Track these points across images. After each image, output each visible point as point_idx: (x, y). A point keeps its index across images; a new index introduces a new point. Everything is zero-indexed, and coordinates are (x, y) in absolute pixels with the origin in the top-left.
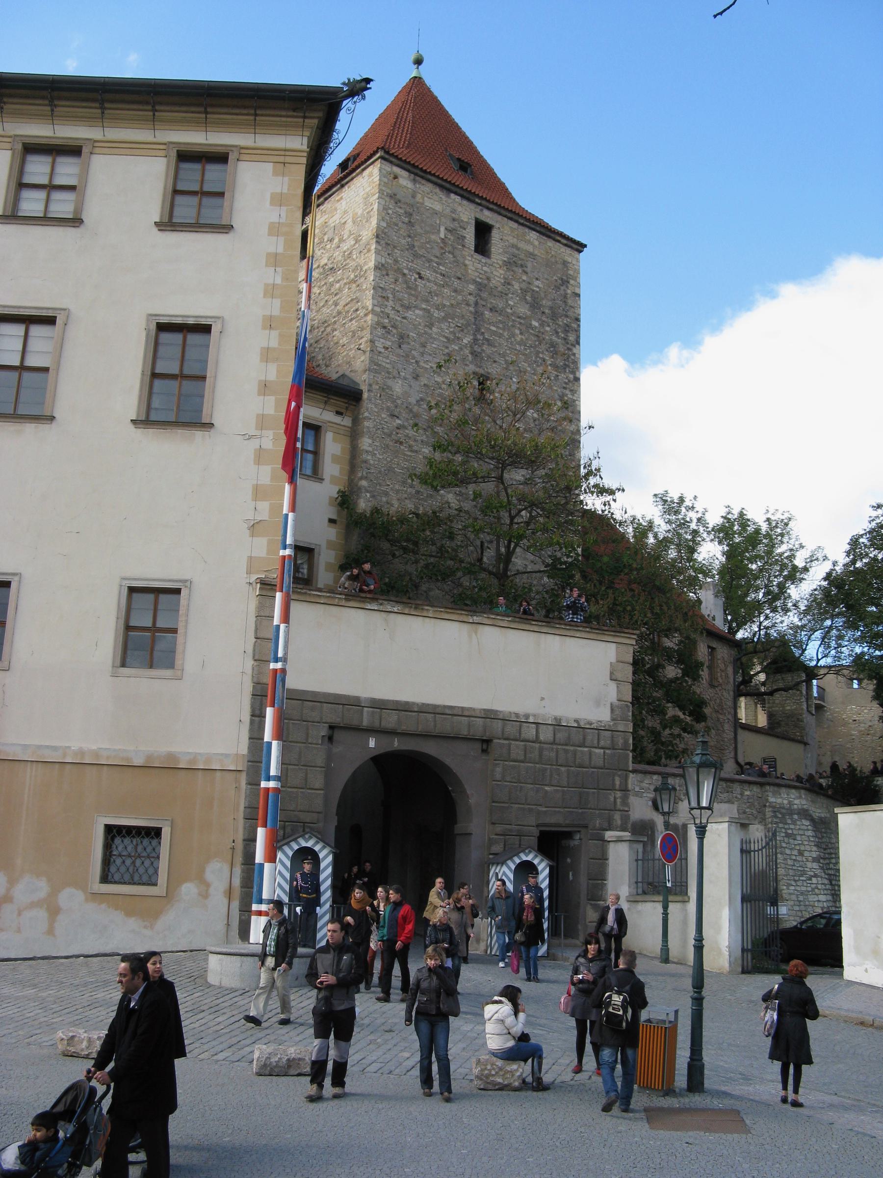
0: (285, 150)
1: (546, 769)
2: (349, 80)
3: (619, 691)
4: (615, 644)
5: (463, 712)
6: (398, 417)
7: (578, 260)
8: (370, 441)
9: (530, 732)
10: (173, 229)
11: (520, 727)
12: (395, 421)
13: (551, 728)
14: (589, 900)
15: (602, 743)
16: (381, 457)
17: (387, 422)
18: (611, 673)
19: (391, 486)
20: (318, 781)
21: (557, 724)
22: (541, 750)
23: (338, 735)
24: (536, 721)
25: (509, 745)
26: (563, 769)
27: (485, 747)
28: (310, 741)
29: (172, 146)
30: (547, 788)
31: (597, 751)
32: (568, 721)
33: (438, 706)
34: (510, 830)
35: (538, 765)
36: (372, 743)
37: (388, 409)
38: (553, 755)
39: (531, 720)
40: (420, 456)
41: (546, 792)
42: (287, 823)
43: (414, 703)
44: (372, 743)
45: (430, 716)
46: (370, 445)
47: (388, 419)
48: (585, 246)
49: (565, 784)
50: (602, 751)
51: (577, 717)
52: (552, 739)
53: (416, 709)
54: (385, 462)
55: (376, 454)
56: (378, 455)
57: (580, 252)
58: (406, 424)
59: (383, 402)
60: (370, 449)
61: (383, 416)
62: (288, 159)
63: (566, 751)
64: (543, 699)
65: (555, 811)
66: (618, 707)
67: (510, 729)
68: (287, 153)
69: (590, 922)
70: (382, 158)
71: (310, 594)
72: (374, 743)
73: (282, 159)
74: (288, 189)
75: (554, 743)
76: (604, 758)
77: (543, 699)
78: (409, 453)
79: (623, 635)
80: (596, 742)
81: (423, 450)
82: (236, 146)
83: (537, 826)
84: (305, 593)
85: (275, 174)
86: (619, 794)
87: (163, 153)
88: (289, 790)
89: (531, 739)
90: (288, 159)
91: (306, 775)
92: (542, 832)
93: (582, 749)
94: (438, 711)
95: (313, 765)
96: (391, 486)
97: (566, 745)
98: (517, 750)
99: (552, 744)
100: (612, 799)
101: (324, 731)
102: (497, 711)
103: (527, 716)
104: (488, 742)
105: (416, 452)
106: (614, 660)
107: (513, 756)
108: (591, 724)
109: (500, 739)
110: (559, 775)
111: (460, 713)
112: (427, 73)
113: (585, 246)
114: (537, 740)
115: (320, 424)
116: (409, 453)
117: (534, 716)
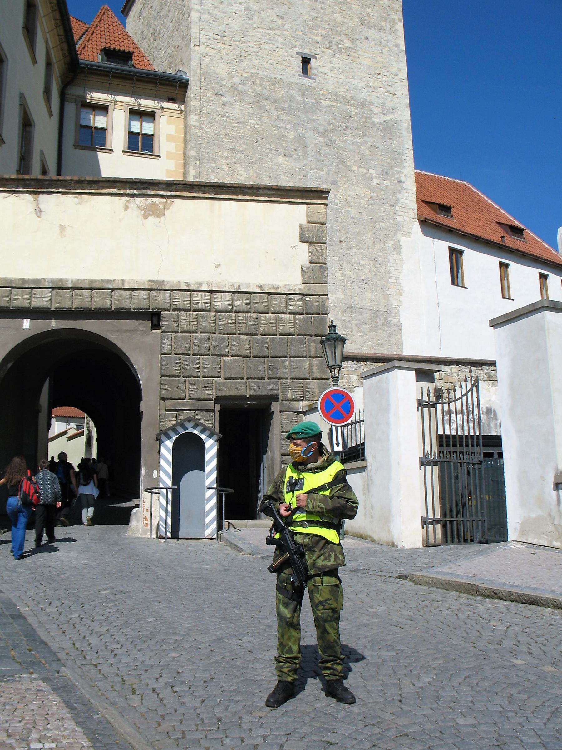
5: (123, 284)
6: (223, 96)
8: (197, 117)
9: (203, 300)
12: (220, 99)
16: (208, 130)
17: (212, 101)
18: (301, 235)
32: (249, 285)
34: (183, 404)
37: (213, 88)
40: (248, 127)
43: (67, 280)
46: (197, 121)
47: (214, 98)
50: (292, 316)
51: (260, 282)
53: (70, 286)
54: (213, 134)
55: (203, 128)
56: (205, 129)
58: (231, 100)
59: (207, 84)
61: (208, 95)
64: (218, 265)
66: (309, 268)
77: (218, 265)
78: (236, 125)
81: (250, 121)
94: (94, 285)
102: (163, 281)
103: (200, 284)
105: (243, 123)
106: (304, 221)
108: (277, 288)
111: (121, 286)
116: (236, 125)
117: (207, 283)
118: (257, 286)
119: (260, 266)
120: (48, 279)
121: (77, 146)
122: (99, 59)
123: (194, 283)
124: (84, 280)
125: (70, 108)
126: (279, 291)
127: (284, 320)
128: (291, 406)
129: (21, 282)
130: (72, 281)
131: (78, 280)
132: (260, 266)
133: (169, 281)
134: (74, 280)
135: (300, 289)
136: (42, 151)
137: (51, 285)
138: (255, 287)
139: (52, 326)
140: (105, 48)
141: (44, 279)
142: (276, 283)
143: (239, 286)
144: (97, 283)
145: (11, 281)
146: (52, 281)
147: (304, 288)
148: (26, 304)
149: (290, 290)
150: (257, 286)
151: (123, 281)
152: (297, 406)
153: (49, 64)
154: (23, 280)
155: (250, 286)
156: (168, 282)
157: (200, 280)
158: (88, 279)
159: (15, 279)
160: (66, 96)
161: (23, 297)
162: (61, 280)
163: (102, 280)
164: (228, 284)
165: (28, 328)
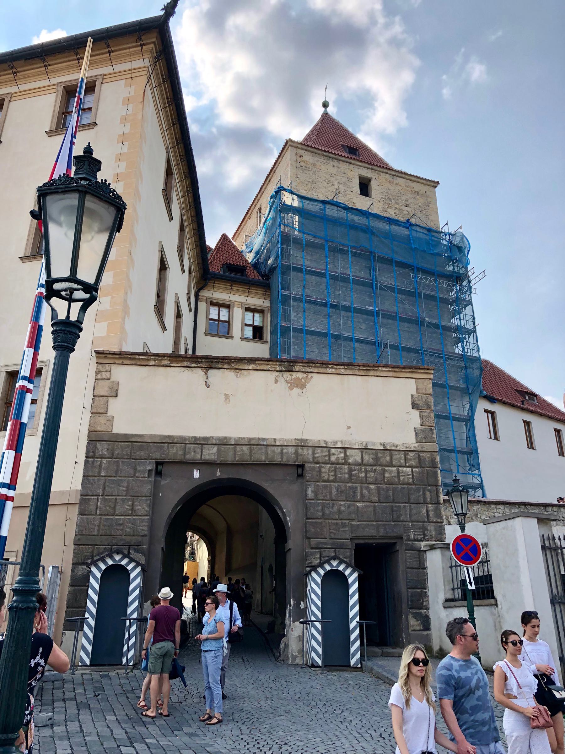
0: (132, 70)
1: (356, 488)
2: (164, 5)
3: (422, 418)
4: (414, 380)
5: (275, 442)
7: (435, 193)
9: (339, 456)
10: (57, 134)
11: (329, 452)
13: (358, 452)
14: (410, 608)
15: (409, 463)
19: (312, 340)
20: (143, 508)
21: (364, 450)
22: (350, 471)
23: (166, 469)
24: (343, 446)
25: (320, 468)
26: (372, 487)
27: (300, 471)
28: (137, 474)
29: (60, 85)
30: (358, 504)
31: (405, 469)
32: (374, 444)
33: (253, 439)
35: (348, 485)
36: (196, 475)
38: (362, 474)
39: (339, 445)
41: (358, 507)
42: (113, 547)
43: (231, 438)
44: (196, 475)
45: (245, 448)
48: (438, 183)
49: (375, 498)
50: (410, 469)
51: (382, 441)
52: (360, 461)
53: (233, 443)
57: (435, 187)
60: (296, 319)
62: (134, 75)
63: (374, 471)
64: (349, 428)
65: (368, 525)
66: (421, 430)
67: (319, 454)
68: (133, 71)
69: (412, 631)
70: (290, 146)
71: (139, 359)
72: (198, 474)
73: (130, 76)
74: (135, 93)
75: (362, 464)
76: (413, 476)
77: (349, 428)
79: (419, 371)
80: (403, 462)
82: (101, 75)
83: (352, 539)
84: (135, 358)
85: (126, 86)
86: (431, 507)
87: (54, 91)
88: (116, 517)
89: (339, 461)
90: (134, 75)
91: (133, 504)
92: (357, 545)
93: (391, 468)
94: (252, 442)
95: (139, 495)
96: (312, 340)
97: (375, 465)
98: (327, 471)
99: (360, 465)
100: (424, 511)
101: (151, 466)
102: (307, 440)
103: (336, 442)
104: (302, 466)
107: (324, 476)
108: (397, 446)
109: (311, 463)
110: (369, 492)
111: (273, 443)
112: (331, 110)
113: (438, 183)
114: (346, 462)
115: (263, 309)
117: (342, 442)
118: (381, 444)
119: (382, 428)
120: (215, 437)
121: (206, 334)
122: (221, 272)
123: (331, 441)
124: (244, 438)
125: (202, 306)
126: (398, 448)
127: (403, 472)
128: (413, 546)
129: (193, 439)
130: (235, 439)
131: (240, 438)
132: (382, 428)
133: (311, 440)
134: (236, 439)
135: (415, 447)
136: (185, 336)
137: (218, 442)
138: (379, 445)
139: (218, 475)
140: (227, 263)
141: (213, 437)
142: (396, 442)
143: (366, 444)
144: (255, 440)
145: (185, 439)
146: (219, 439)
147: (418, 446)
148: (198, 457)
149: (406, 448)
150: (381, 444)
151: (275, 439)
152: (418, 545)
153: (190, 272)
154: (195, 438)
155: (375, 444)
156: (310, 440)
157: (335, 439)
158: (248, 438)
159: (189, 437)
160: (199, 297)
161: (194, 451)
162: (225, 438)
163: (259, 439)
164: (358, 443)
165: (198, 477)
